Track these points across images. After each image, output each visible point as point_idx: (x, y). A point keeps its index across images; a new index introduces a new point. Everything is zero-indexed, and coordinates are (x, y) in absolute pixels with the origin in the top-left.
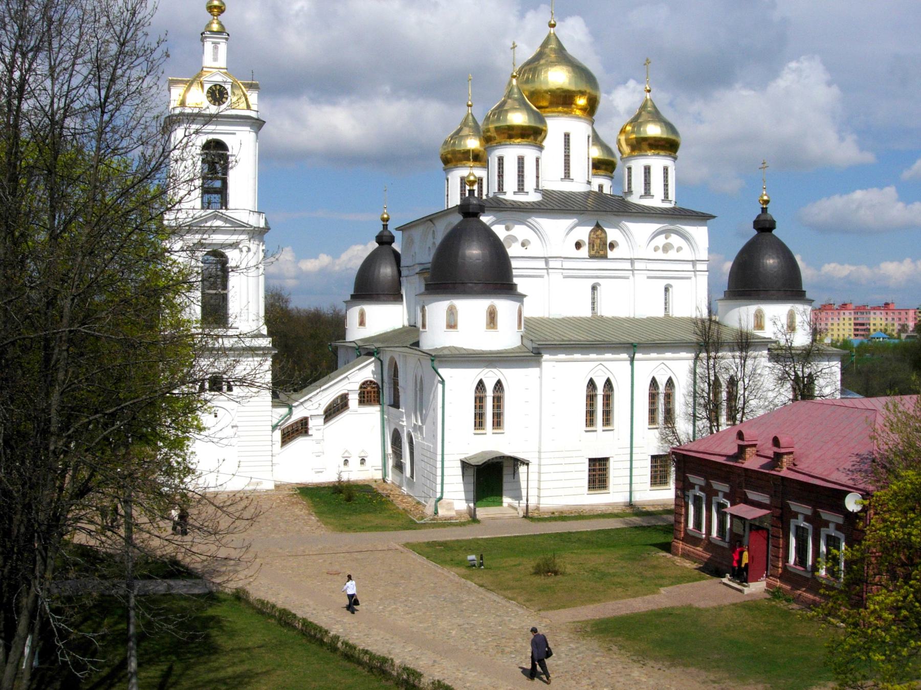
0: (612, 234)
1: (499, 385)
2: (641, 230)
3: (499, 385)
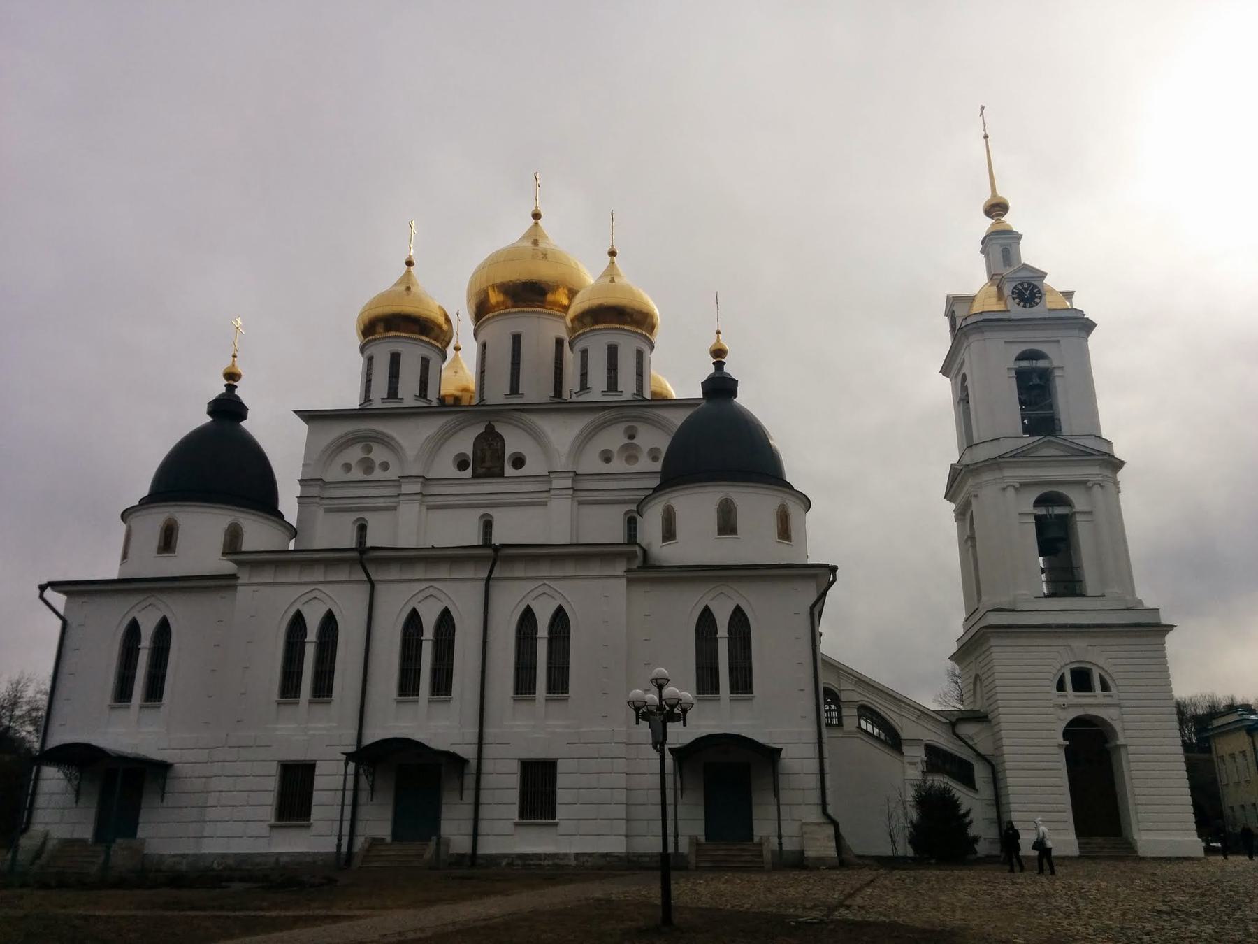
0: (514, 442)
1: (163, 629)
2: (561, 434)
3: (163, 629)
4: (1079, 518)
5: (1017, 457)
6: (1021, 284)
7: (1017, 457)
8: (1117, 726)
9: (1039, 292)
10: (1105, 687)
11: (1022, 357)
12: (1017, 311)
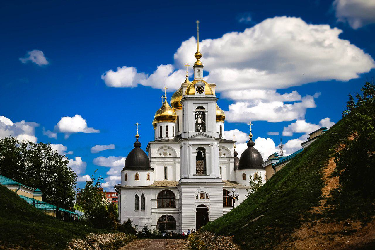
4: (207, 154)
5: (193, 138)
6: (199, 86)
7: (193, 138)
8: (209, 207)
9: (204, 89)
10: (207, 197)
11: (198, 108)
12: (198, 95)
